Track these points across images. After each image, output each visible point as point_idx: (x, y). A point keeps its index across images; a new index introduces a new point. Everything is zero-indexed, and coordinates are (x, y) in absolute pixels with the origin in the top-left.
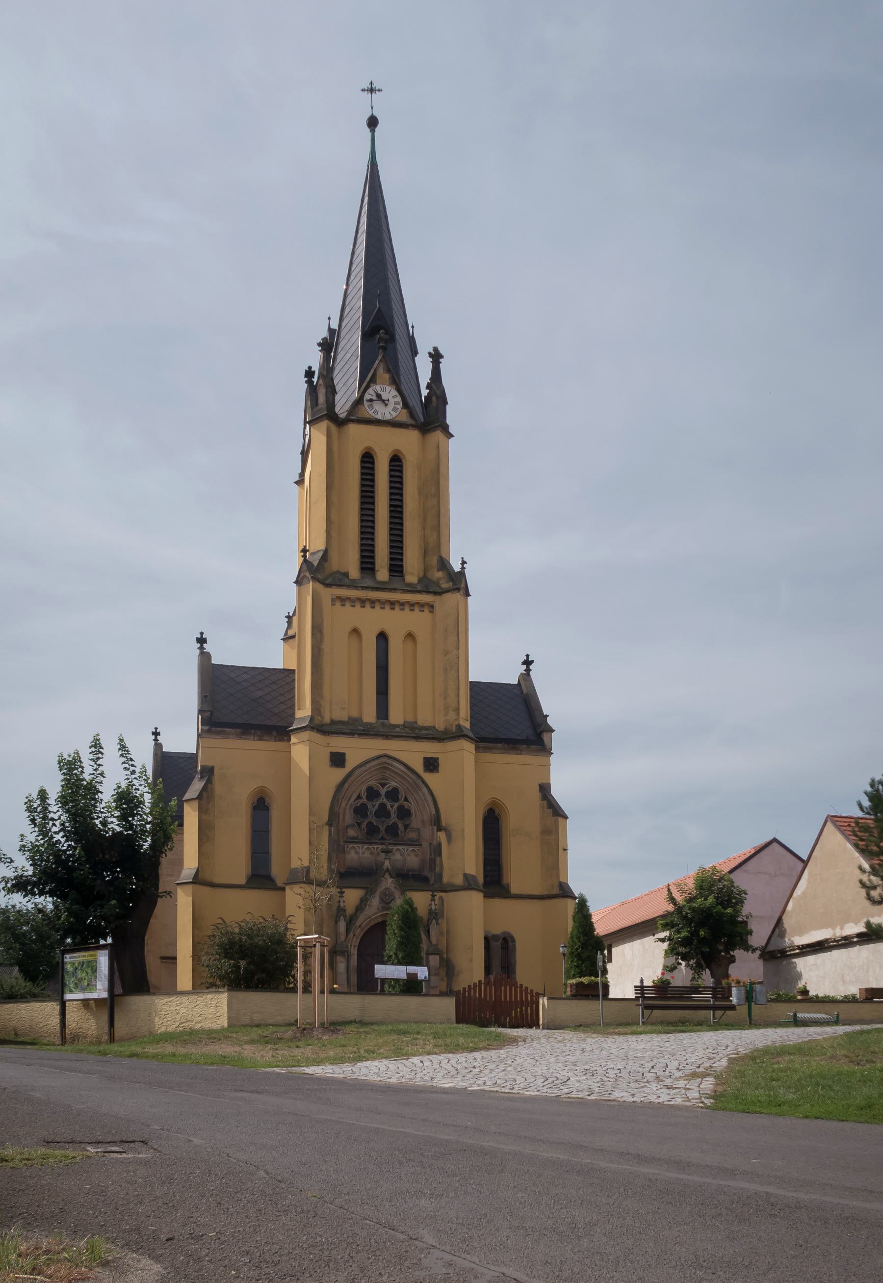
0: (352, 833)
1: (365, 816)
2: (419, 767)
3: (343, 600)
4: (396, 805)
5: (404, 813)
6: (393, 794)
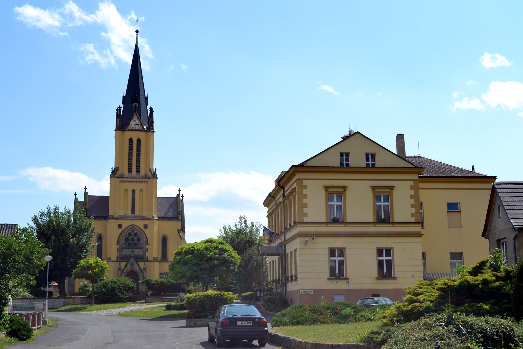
0: (124, 246)
1: (128, 241)
2: (142, 227)
3: (123, 182)
5: (139, 240)
6: (136, 234)
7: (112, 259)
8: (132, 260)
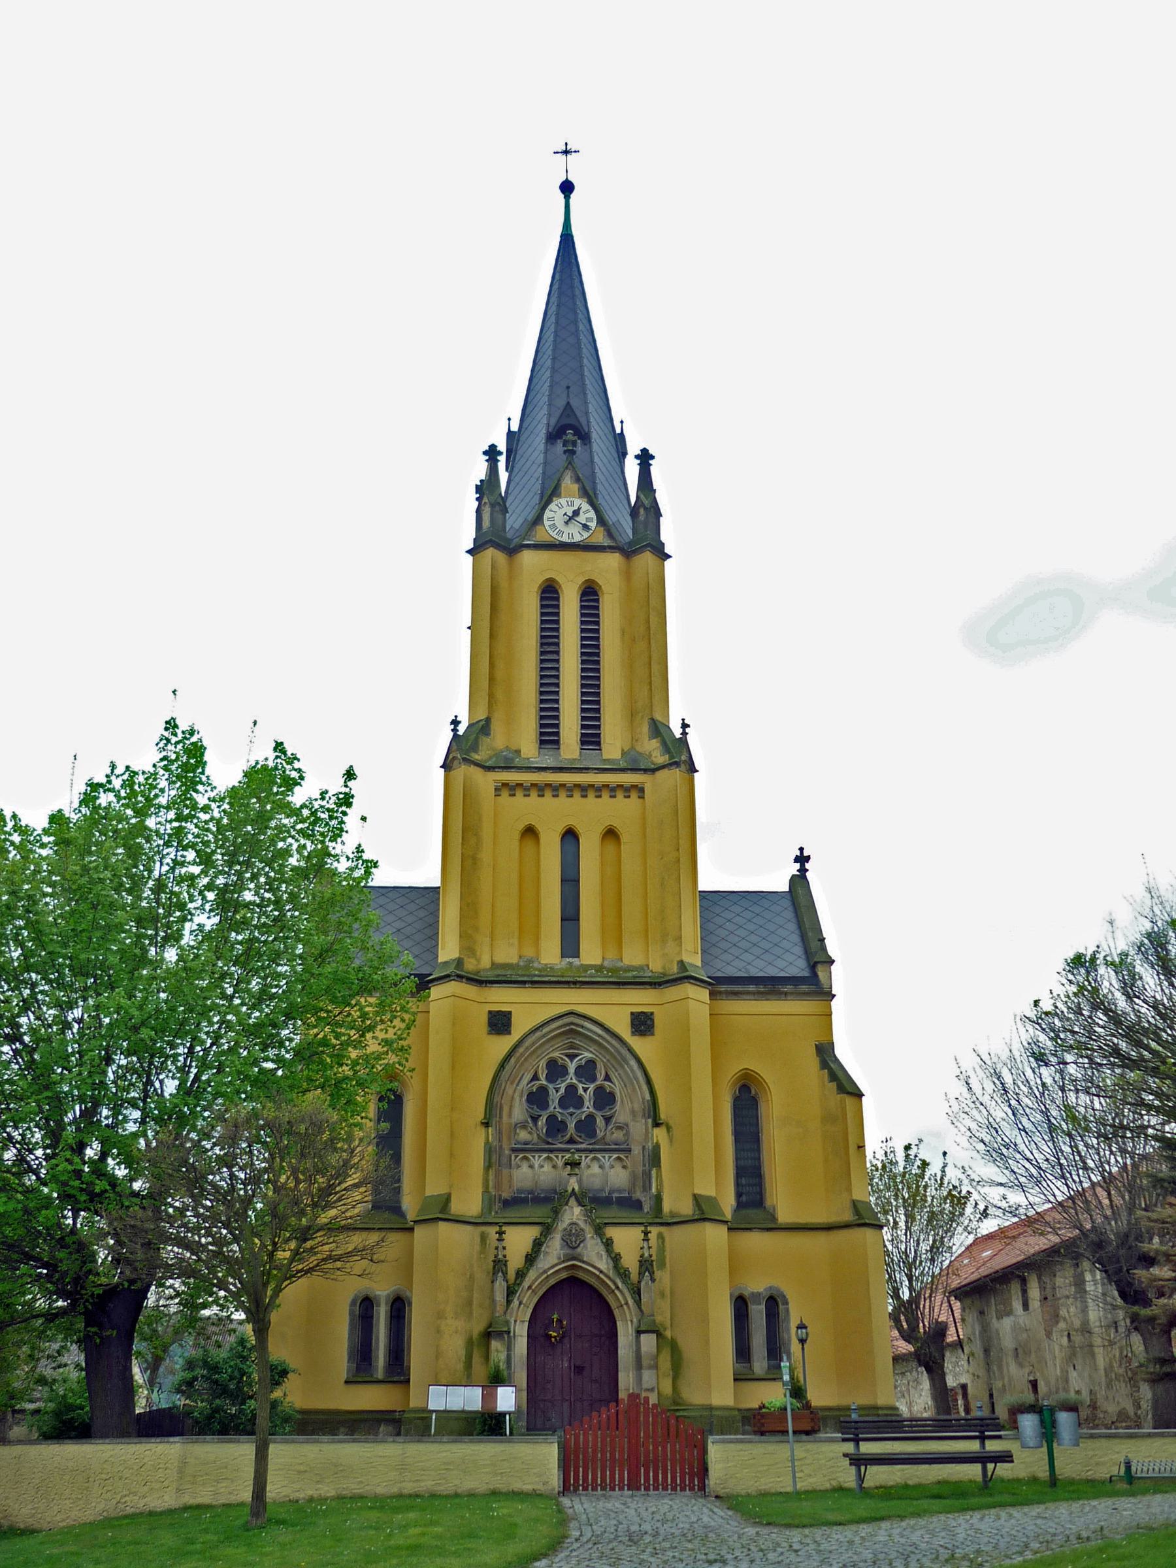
0: (523, 1135)
1: (544, 1105)
2: (623, 1028)
3: (512, 788)
4: (592, 1087)
5: (605, 1099)
7: (456, 1208)
8: (574, 1213)
